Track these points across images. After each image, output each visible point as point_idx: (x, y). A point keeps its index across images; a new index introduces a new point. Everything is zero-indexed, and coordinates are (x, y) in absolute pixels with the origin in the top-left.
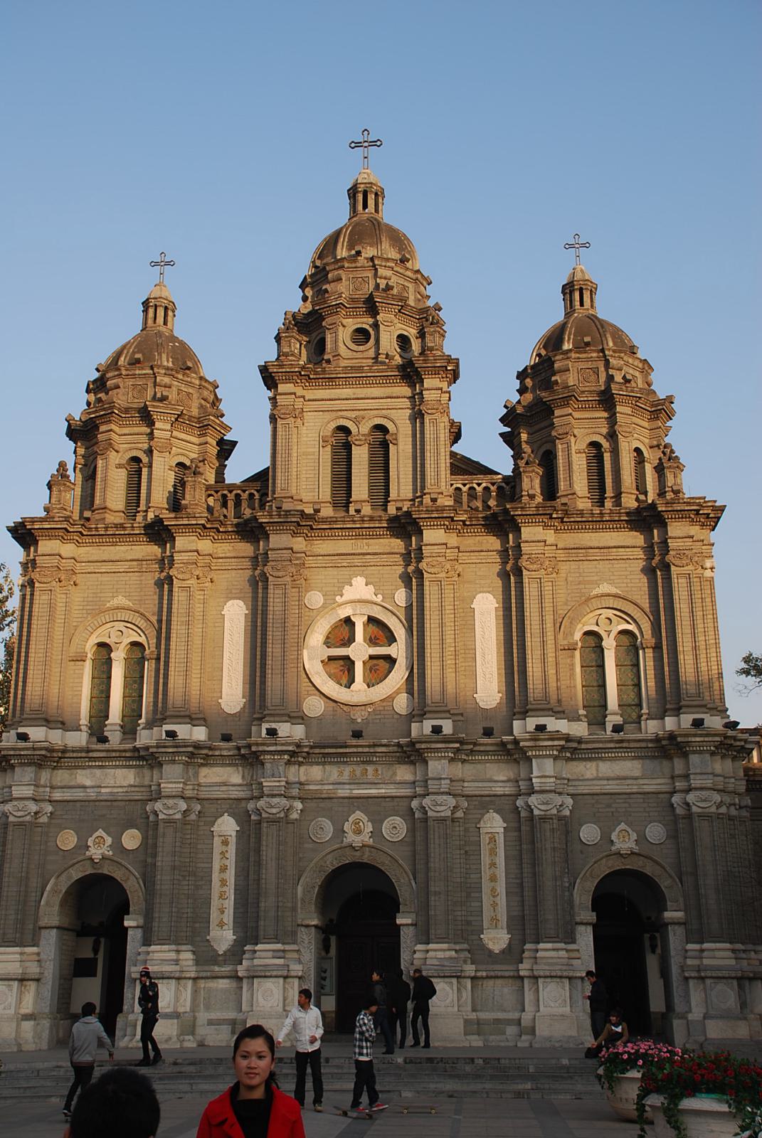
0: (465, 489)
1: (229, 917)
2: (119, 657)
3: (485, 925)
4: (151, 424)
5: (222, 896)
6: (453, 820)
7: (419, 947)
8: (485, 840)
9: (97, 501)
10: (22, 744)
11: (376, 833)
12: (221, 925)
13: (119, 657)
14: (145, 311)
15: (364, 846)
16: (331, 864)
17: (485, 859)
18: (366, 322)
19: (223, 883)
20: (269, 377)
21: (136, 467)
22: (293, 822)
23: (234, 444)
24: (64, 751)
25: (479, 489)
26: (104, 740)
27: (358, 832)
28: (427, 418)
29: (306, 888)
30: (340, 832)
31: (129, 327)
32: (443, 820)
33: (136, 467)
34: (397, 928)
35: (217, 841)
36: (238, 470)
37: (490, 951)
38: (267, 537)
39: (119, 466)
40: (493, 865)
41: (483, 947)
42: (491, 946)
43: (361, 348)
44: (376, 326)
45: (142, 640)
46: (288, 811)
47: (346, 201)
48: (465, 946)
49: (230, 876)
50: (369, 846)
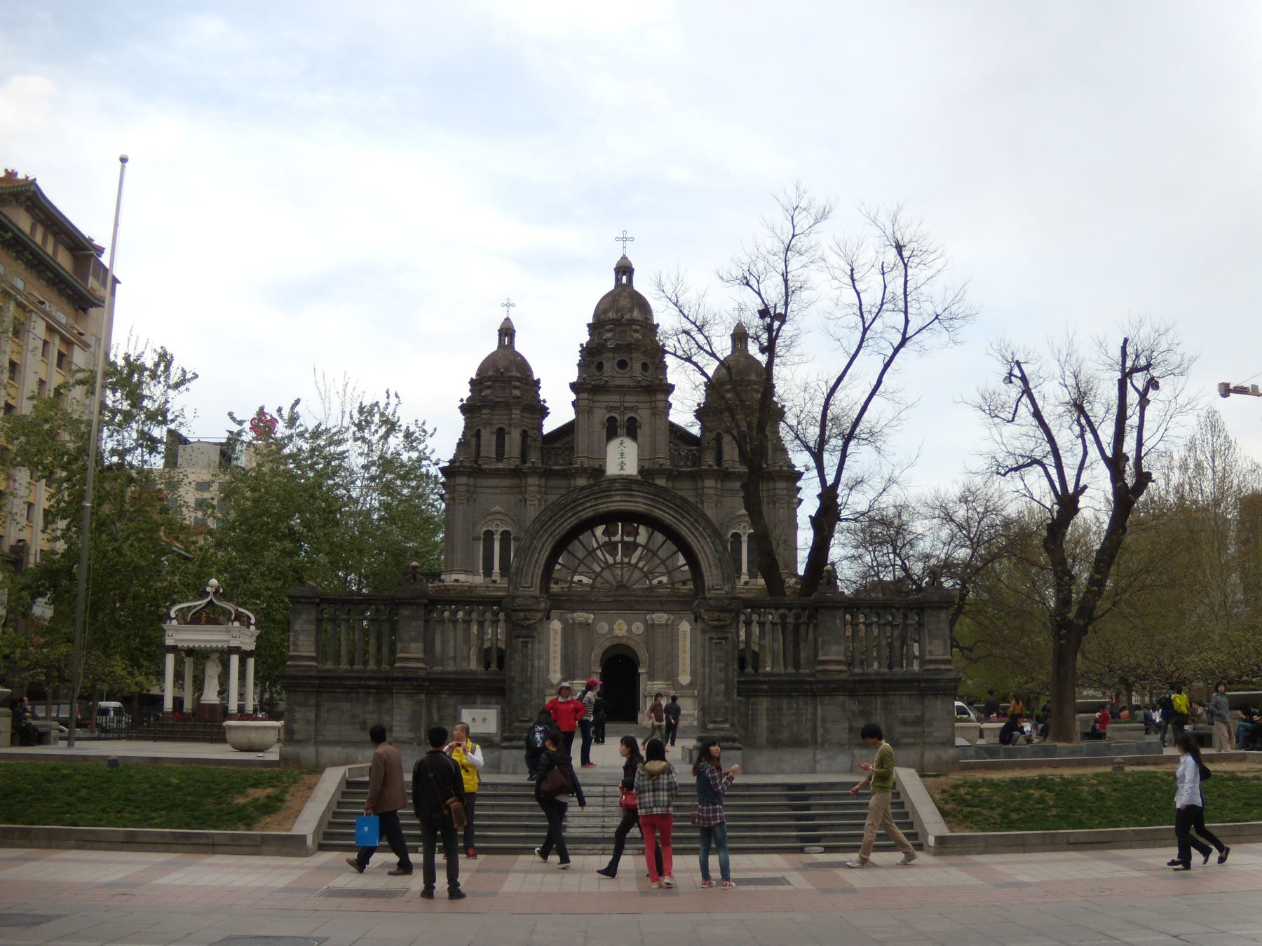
0: (676, 453)
1: (558, 668)
2: (497, 537)
3: (680, 672)
4: (511, 410)
5: (555, 658)
6: (667, 625)
7: (649, 683)
8: (681, 634)
9: (483, 454)
10: (456, 584)
11: (629, 630)
12: (555, 671)
13: (497, 537)
14: (500, 335)
15: (623, 637)
16: (607, 644)
17: (681, 643)
18: (625, 357)
19: (555, 652)
20: (574, 387)
21: (501, 434)
22: (588, 624)
23: (549, 413)
24: (476, 587)
25: (683, 454)
26: (494, 582)
27: (621, 630)
28: (657, 416)
29: (597, 654)
30: (611, 629)
31: (492, 345)
32: (661, 625)
33: (501, 434)
34: (639, 674)
35: (551, 632)
36: (549, 426)
37: (682, 685)
38: (575, 479)
39: (492, 433)
40: (684, 645)
41: (678, 682)
42: (682, 682)
43: (623, 371)
44: (631, 359)
45: (509, 529)
46: (587, 619)
47: (613, 273)
48: (671, 682)
49: (559, 648)
50: (626, 637)
